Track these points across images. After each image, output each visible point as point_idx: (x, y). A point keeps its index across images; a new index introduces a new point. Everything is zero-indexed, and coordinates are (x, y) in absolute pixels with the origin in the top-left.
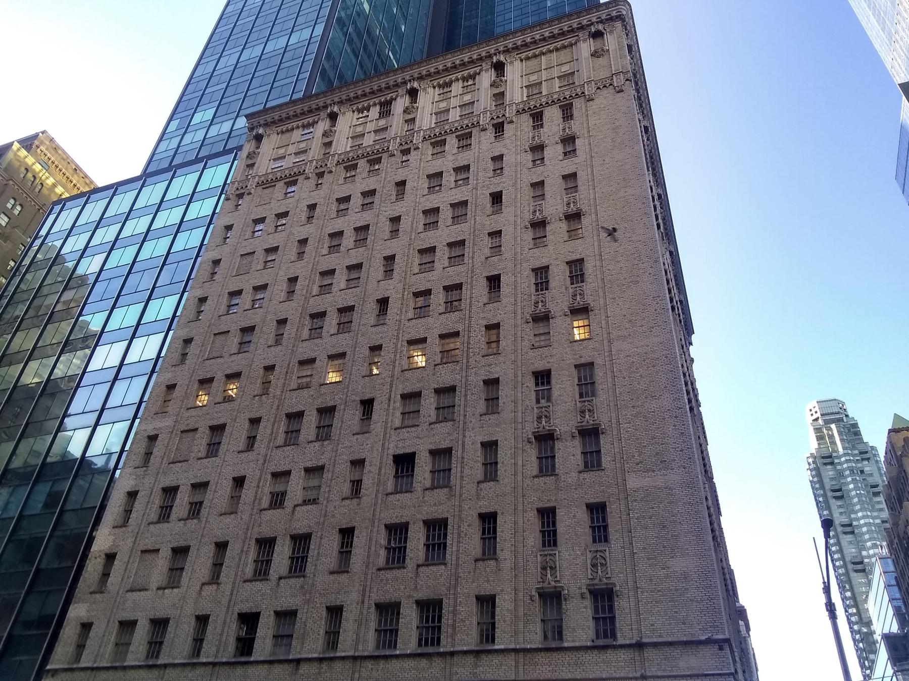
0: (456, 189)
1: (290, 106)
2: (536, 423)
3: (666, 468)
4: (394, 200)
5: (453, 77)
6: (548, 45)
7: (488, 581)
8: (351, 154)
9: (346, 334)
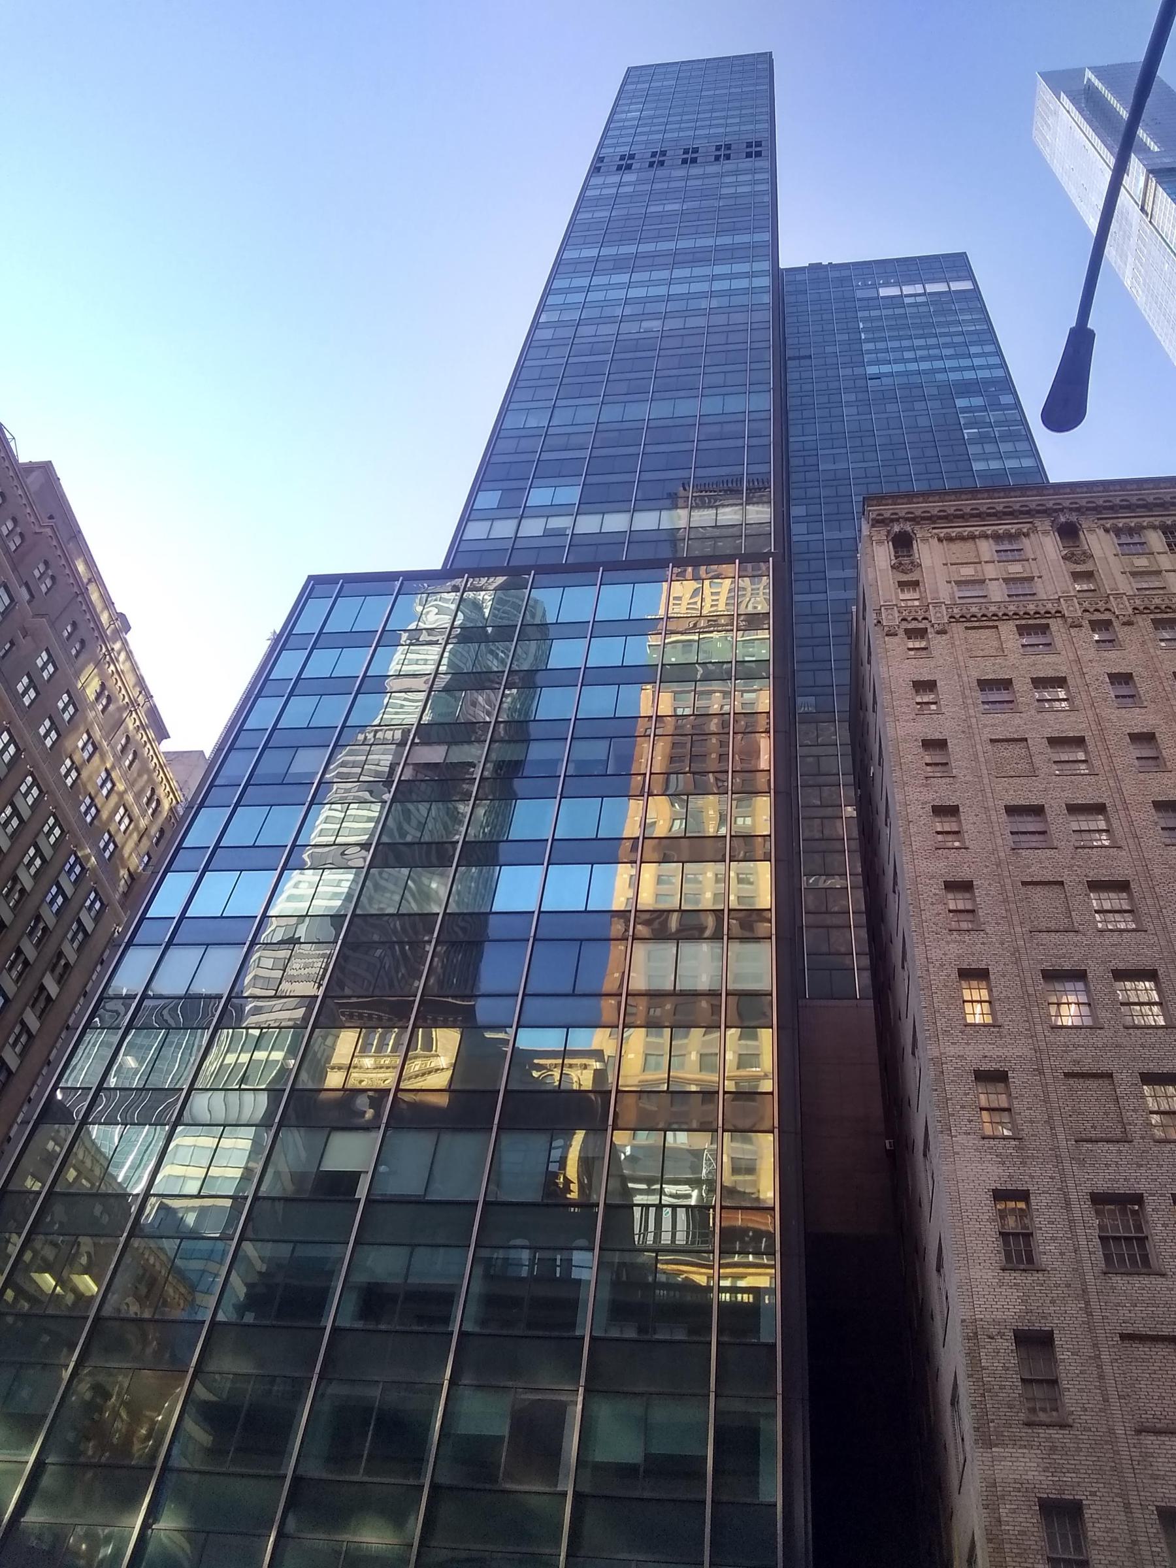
1: (964, 497)
6: (1152, 516)
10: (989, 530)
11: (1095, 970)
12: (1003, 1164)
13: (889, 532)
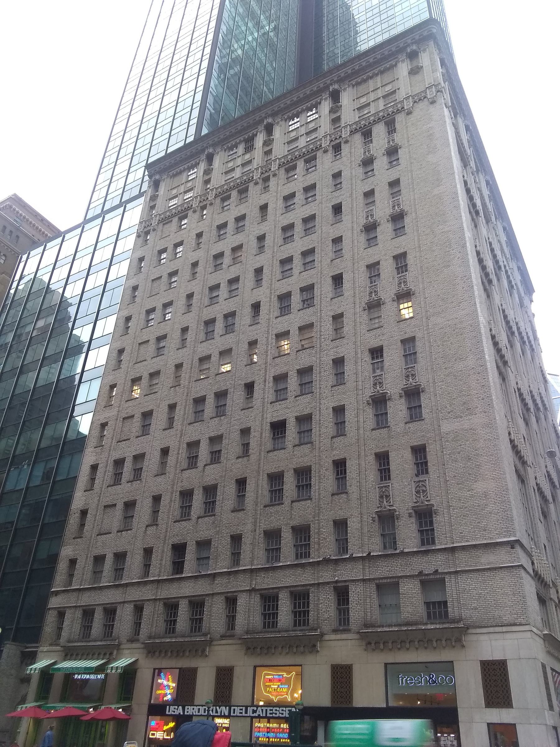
0: (306, 206)
2: (372, 388)
3: (471, 414)
4: (260, 221)
5: (299, 109)
7: (341, 509)
8: (225, 187)
9: (231, 334)
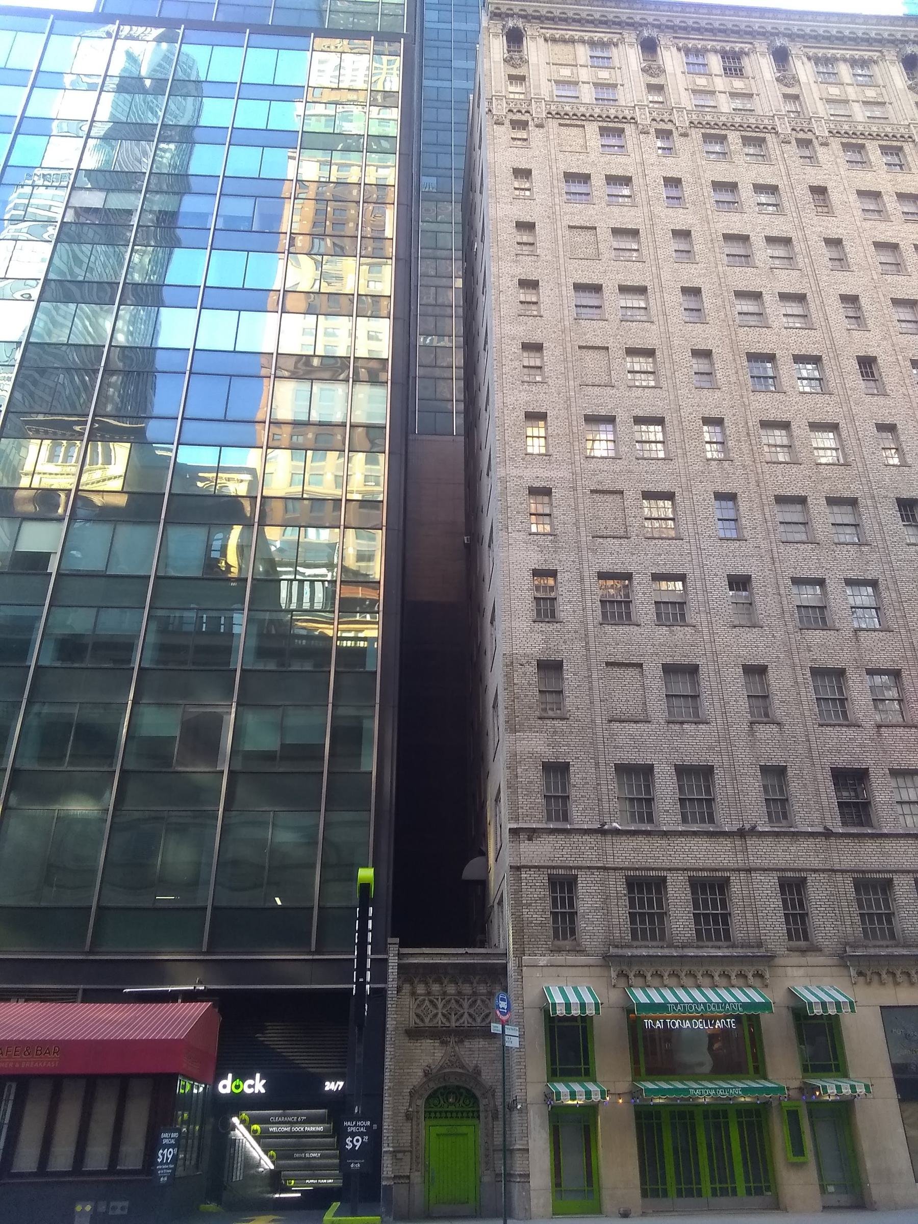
10: (587, 36)
11: (623, 417)
12: (542, 552)
13: (504, 26)
